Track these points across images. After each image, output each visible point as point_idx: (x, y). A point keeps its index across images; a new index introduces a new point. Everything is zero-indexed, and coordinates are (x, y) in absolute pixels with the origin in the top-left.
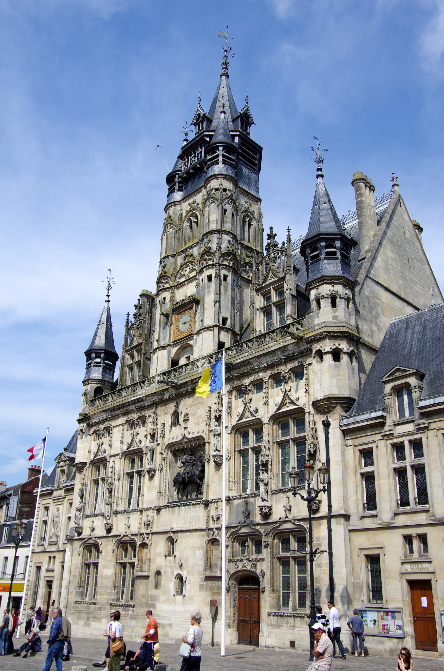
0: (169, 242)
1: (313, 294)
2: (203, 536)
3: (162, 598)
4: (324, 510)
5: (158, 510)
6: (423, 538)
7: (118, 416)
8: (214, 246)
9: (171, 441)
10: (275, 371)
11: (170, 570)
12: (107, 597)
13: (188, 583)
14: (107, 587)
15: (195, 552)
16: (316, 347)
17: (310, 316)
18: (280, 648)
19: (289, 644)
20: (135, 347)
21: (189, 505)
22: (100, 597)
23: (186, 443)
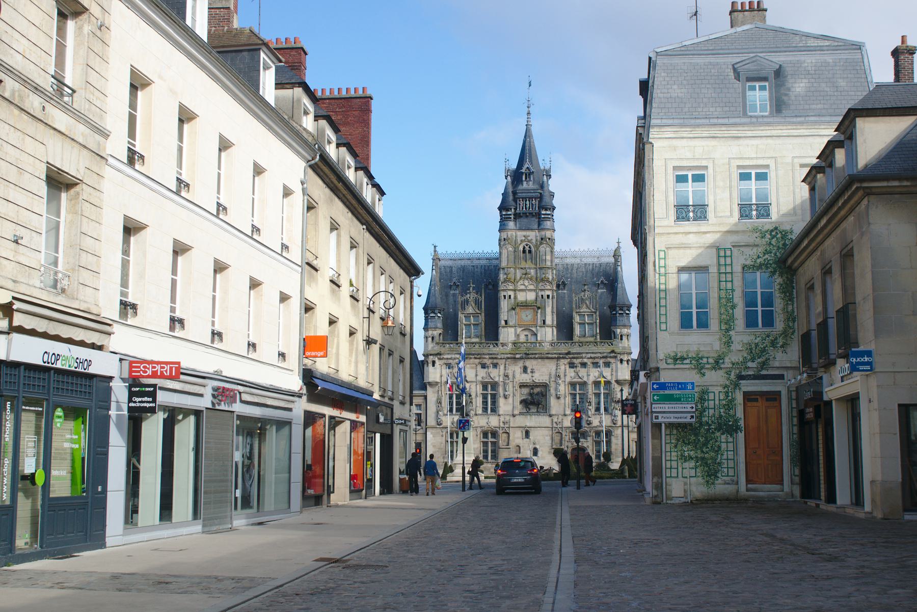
1: (619, 331)
8: (551, 278)
16: (619, 357)
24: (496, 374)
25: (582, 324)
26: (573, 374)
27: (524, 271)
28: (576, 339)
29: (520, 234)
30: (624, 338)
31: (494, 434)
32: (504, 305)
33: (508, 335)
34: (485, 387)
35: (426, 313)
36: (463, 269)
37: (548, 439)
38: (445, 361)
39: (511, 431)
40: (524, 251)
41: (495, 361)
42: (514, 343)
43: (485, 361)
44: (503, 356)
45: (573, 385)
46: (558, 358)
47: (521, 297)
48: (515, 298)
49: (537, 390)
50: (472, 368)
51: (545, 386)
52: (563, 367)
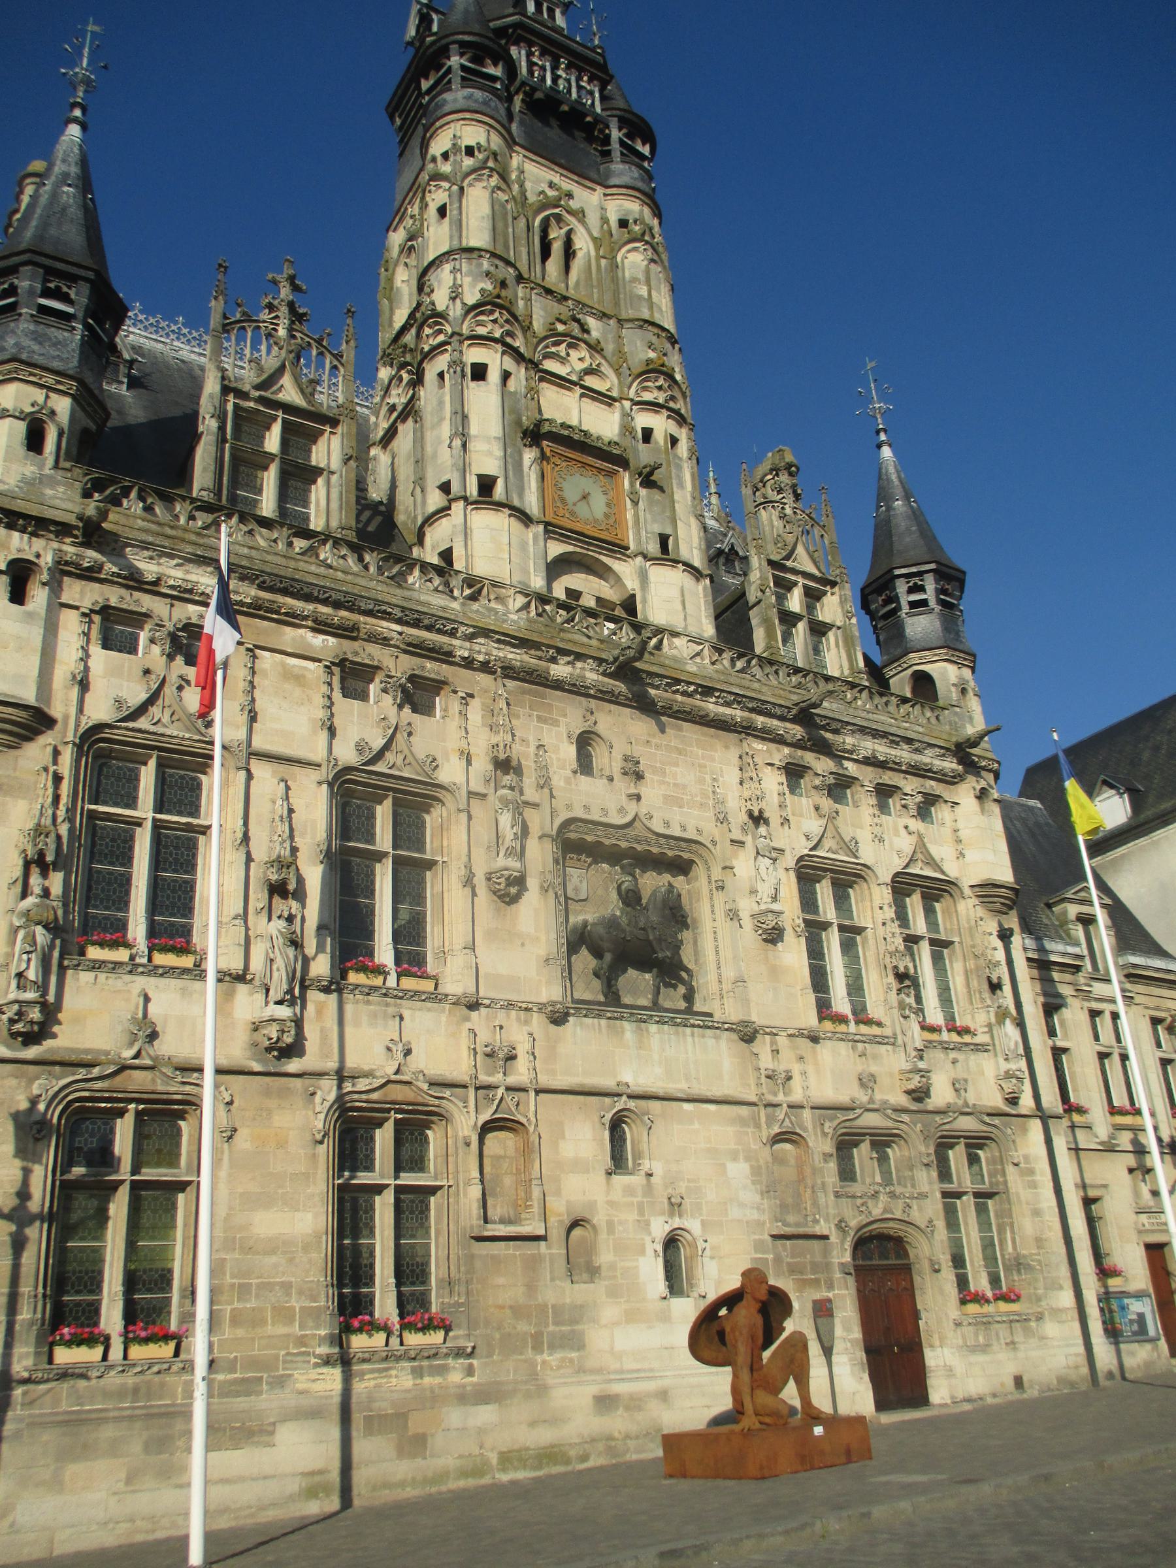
0: (500, 225)
2: (742, 1122)
3: (610, 1312)
4: (1027, 1102)
7: (292, 619)
9: (579, 813)
10: (888, 778)
11: (632, 1216)
12: (296, 1329)
13: (712, 1258)
14: (287, 1287)
15: (724, 1165)
17: (956, 714)
18: (994, 1395)
19: (1010, 1383)
20: (288, 408)
21: (678, 1025)
22: (240, 1332)
23: (636, 840)
26: (814, 826)
27: (563, 310)
37: (739, 1170)
38: (114, 596)
41: (431, 668)
44: (484, 649)
46: (747, 730)
47: (562, 407)
50: (298, 679)
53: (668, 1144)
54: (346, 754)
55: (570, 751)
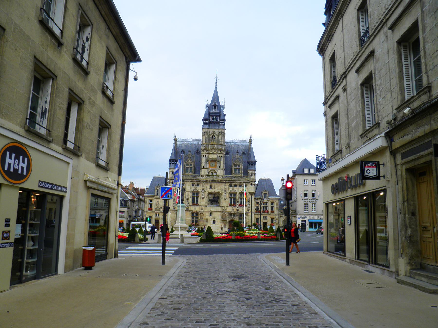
4: (250, 211)
5: (206, 206)
6: (266, 216)
8: (223, 149)
24: (199, 189)
25: (235, 169)
28: (233, 175)
29: (211, 131)
30: (253, 175)
31: (197, 214)
32: (203, 159)
33: (204, 172)
34: (194, 194)
35: (170, 162)
36: (187, 145)
39: (204, 213)
40: (212, 138)
42: (207, 176)
43: (194, 183)
45: (231, 194)
46: (225, 183)
47: (211, 156)
48: (208, 157)
49: (216, 196)
51: (219, 194)
52: (227, 187)
53: (214, 215)
54: (192, 190)
55: (209, 187)
